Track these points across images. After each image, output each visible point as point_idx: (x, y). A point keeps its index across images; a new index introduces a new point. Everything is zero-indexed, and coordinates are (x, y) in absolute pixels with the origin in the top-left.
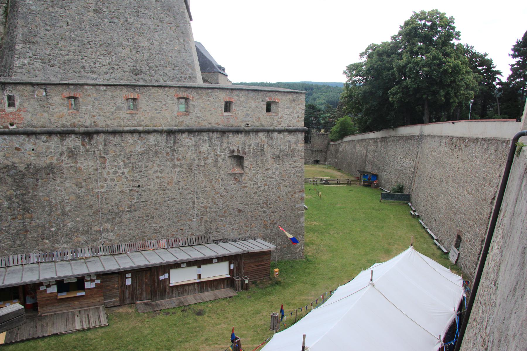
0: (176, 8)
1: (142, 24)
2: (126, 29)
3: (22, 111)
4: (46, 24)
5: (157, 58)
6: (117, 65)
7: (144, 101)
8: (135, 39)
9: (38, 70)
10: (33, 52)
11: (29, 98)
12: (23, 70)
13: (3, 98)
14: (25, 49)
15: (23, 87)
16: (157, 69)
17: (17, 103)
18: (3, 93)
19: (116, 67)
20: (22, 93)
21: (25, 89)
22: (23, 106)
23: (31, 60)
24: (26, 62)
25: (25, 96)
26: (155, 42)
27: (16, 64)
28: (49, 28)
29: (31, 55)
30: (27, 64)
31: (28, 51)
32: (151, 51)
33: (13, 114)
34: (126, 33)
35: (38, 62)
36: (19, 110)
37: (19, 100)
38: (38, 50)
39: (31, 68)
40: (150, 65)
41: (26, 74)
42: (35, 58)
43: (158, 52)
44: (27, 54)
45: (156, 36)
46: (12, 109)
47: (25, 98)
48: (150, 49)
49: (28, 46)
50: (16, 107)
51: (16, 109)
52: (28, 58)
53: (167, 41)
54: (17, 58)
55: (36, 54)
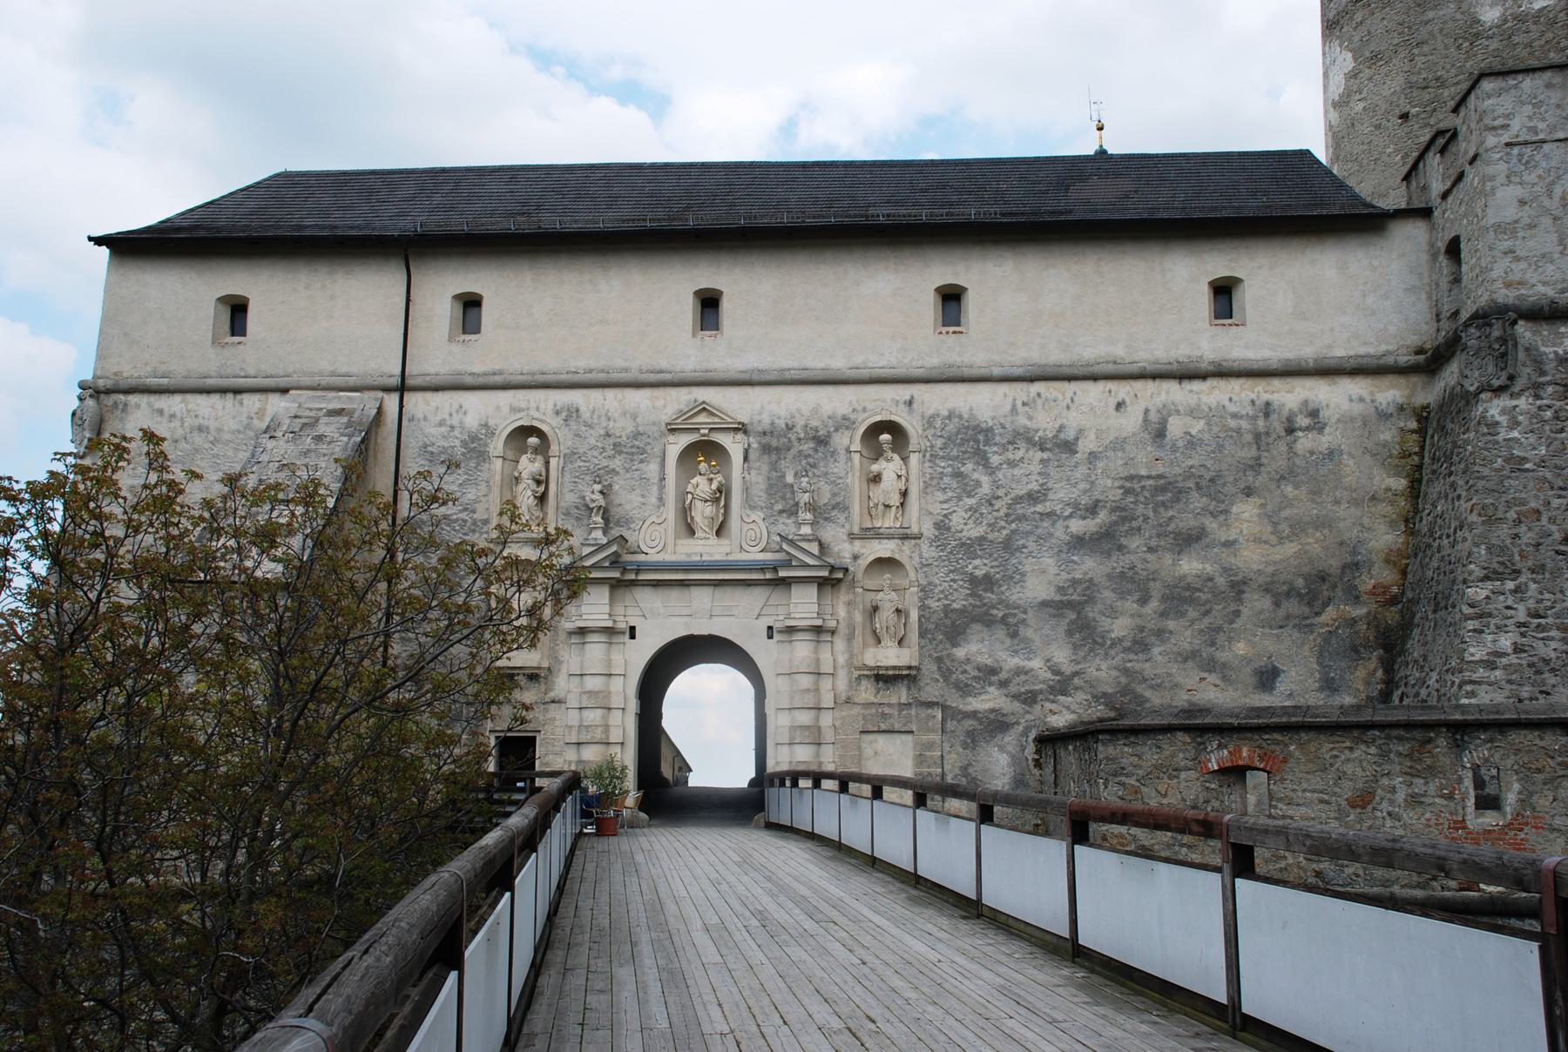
3: (1526, 824)
9: (1552, 670)
10: (1531, 604)
11: (1552, 780)
12: (1498, 673)
13: (1460, 780)
14: (1502, 598)
15: (1530, 737)
17: (1511, 798)
18: (1459, 757)
20: (1526, 759)
21: (1542, 743)
22: (1534, 809)
23: (1523, 635)
24: (1505, 642)
25: (1539, 771)
27: (1472, 655)
29: (1521, 616)
30: (1510, 651)
31: (1510, 603)
33: (1494, 836)
35: (1553, 639)
36: (1517, 823)
37: (1516, 786)
38: (1547, 596)
39: (1524, 662)
41: (1509, 687)
42: (1539, 625)
44: (1510, 612)
46: (1490, 819)
47: (1540, 777)
49: (1510, 585)
50: (1508, 809)
51: (1504, 815)
52: (1512, 628)
54: (1474, 631)
55: (1541, 612)
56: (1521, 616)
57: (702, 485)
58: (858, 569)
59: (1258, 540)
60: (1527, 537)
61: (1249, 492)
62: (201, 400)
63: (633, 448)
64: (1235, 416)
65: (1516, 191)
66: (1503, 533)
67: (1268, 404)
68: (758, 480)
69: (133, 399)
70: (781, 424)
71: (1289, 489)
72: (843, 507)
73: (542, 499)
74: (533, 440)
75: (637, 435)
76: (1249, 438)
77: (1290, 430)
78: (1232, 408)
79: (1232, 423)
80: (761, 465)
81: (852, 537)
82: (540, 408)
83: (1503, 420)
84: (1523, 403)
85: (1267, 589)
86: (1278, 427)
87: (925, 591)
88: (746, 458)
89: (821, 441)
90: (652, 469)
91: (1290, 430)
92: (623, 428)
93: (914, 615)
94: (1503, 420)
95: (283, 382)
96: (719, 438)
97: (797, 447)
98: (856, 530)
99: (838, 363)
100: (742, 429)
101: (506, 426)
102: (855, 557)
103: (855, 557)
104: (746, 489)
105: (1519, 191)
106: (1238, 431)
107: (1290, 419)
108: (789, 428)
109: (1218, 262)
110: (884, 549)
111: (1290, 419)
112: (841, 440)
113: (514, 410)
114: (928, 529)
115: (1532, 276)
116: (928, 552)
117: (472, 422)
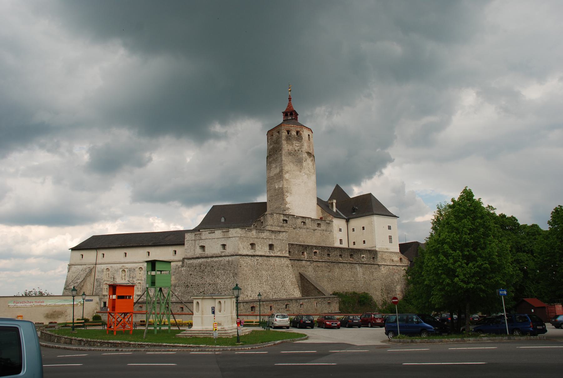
0: (235, 262)
1: (219, 273)
2: (212, 276)
4: (186, 279)
5: (223, 287)
6: (206, 292)
7: (185, 308)
8: (215, 280)
16: (221, 292)
19: (205, 293)
26: (223, 280)
28: (186, 280)
29: (179, 291)
32: (221, 285)
34: (212, 278)
40: (219, 291)
43: (224, 285)
45: (224, 277)
48: (220, 284)
53: (229, 279)
56: (179, 291)
57: (123, 275)
58: (137, 284)
59: (174, 280)
60: (181, 283)
61: (174, 275)
62: (79, 266)
63: (117, 271)
64: (174, 266)
65: (187, 245)
66: (180, 282)
67: (177, 265)
68: (128, 274)
69: (73, 266)
70: (131, 268)
71: (177, 275)
72: (136, 277)
73: (109, 276)
74: (108, 270)
75: (117, 269)
76: (175, 269)
77: (179, 268)
78: (174, 265)
79: (173, 267)
80: (129, 272)
81: (136, 280)
82: (109, 266)
83: (183, 270)
84: (185, 268)
85: (174, 286)
86: (178, 267)
87: (143, 286)
88: (127, 272)
89: (134, 270)
90: (119, 273)
91: (179, 268)
92: (116, 268)
93: (141, 289)
94: (183, 270)
95: (85, 264)
96: (125, 269)
97: (132, 270)
98: (137, 279)
99: (137, 261)
100: (127, 268)
101: (106, 268)
102: (137, 282)
103: (137, 282)
104: (127, 275)
105: (187, 245)
106: (174, 268)
107: (179, 266)
108: (132, 268)
109: (174, 248)
110: (139, 281)
111: (179, 266)
112: (136, 269)
113: (106, 266)
114: (144, 280)
115: (188, 255)
116: (143, 282)
117: (102, 268)
